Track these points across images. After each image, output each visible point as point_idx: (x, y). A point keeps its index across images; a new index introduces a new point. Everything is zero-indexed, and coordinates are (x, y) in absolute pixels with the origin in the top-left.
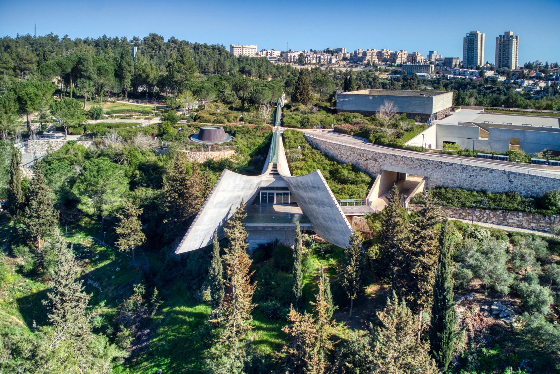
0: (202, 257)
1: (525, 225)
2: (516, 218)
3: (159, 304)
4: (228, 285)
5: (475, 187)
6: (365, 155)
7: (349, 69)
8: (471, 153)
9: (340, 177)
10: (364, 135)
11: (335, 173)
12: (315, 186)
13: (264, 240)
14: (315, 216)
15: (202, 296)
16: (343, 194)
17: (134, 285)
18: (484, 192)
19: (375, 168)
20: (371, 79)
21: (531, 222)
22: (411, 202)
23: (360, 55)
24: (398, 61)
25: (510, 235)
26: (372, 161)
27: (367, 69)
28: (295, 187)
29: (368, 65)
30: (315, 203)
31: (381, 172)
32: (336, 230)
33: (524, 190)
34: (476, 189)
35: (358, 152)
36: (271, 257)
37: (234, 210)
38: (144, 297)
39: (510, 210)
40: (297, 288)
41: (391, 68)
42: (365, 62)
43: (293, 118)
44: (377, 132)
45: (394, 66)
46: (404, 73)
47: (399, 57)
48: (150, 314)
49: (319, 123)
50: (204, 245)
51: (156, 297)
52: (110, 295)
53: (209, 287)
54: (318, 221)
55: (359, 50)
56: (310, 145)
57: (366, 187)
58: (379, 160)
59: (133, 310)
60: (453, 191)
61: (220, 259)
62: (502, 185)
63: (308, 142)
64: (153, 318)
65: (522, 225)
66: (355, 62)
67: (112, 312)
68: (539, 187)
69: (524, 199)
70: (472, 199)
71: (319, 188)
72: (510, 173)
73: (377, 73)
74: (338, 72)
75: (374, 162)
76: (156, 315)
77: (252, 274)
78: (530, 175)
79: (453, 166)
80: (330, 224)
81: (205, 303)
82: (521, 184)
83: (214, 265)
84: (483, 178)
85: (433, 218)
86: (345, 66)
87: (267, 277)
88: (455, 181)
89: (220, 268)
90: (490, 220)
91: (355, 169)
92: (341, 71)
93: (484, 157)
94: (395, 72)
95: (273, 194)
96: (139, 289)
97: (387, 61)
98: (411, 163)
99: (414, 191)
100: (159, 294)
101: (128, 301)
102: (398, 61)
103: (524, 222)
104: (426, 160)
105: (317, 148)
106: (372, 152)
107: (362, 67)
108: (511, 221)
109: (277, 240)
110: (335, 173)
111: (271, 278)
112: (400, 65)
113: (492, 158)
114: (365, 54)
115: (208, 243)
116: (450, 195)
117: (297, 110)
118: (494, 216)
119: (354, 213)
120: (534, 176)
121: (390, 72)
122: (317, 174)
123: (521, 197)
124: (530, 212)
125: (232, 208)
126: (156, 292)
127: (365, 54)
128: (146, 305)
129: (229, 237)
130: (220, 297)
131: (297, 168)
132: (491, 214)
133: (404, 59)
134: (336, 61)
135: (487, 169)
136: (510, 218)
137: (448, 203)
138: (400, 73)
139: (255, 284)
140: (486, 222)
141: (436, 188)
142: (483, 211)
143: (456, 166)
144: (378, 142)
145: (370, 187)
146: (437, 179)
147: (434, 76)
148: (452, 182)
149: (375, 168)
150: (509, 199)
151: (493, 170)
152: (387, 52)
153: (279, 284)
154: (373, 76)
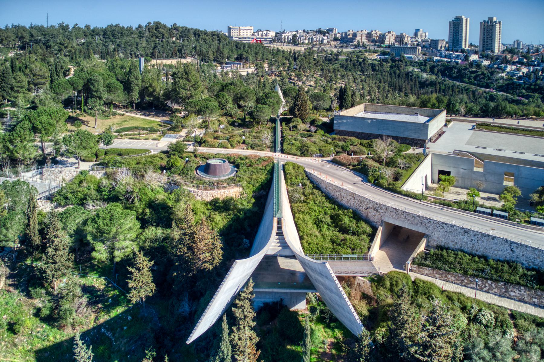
1: (527, 299)
2: (518, 292)
5: (477, 251)
6: (366, 203)
7: (340, 50)
8: (471, 207)
9: (342, 224)
10: (361, 170)
11: (336, 219)
16: (345, 247)
18: (485, 258)
20: (361, 60)
21: (532, 297)
22: (413, 262)
24: (387, 42)
25: (513, 316)
27: (357, 50)
31: (383, 223)
33: (526, 261)
34: (478, 253)
39: (512, 283)
42: (355, 43)
43: (293, 144)
44: (376, 170)
45: (382, 47)
46: (392, 55)
47: (388, 38)
49: (318, 152)
55: (349, 31)
56: (311, 182)
57: (368, 240)
60: (454, 254)
62: (504, 253)
63: (309, 179)
65: (523, 299)
66: (346, 43)
68: (541, 260)
69: (526, 272)
70: (474, 266)
72: (512, 243)
73: (367, 54)
74: (329, 52)
78: (532, 248)
79: (455, 228)
82: (523, 255)
83: (223, 348)
84: (484, 244)
86: (336, 47)
88: (456, 243)
90: (492, 290)
91: (357, 216)
92: (332, 52)
93: (484, 213)
94: (384, 53)
97: (376, 42)
98: (412, 219)
99: (416, 250)
102: (387, 42)
103: (526, 296)
104: (427, 219)
105: (317, 188)
106: (373, 202)
107: (353, 47)
108: (512, 294)
109: (281, 299)
110: (336, 219)
112: (389, 47)
113: (492, 214)
114: (355, 35)
116: (451, 259)
117: (295, 127)
118: (496, 287)
119: (356, 273)
120: (535, 249)
121: (379, 53)
123: (523, 268)
124: (532, 288)
127: (355, 35)
131: (299, 211)
132: (493, 285)
133: (392, 41)
134: (328, 42)
135: (489, 236)
136: (512, 291)
138: (388, 54)
140: (487, 292)
142: (485, 281)
143: (458, 228)
145: (371, 240)
146: (438, 238)
147: (421, 58)
148: (453, 243)
150: (511, 271)
151: (495, 237)
152: (376, 33)
154: (363, 57)
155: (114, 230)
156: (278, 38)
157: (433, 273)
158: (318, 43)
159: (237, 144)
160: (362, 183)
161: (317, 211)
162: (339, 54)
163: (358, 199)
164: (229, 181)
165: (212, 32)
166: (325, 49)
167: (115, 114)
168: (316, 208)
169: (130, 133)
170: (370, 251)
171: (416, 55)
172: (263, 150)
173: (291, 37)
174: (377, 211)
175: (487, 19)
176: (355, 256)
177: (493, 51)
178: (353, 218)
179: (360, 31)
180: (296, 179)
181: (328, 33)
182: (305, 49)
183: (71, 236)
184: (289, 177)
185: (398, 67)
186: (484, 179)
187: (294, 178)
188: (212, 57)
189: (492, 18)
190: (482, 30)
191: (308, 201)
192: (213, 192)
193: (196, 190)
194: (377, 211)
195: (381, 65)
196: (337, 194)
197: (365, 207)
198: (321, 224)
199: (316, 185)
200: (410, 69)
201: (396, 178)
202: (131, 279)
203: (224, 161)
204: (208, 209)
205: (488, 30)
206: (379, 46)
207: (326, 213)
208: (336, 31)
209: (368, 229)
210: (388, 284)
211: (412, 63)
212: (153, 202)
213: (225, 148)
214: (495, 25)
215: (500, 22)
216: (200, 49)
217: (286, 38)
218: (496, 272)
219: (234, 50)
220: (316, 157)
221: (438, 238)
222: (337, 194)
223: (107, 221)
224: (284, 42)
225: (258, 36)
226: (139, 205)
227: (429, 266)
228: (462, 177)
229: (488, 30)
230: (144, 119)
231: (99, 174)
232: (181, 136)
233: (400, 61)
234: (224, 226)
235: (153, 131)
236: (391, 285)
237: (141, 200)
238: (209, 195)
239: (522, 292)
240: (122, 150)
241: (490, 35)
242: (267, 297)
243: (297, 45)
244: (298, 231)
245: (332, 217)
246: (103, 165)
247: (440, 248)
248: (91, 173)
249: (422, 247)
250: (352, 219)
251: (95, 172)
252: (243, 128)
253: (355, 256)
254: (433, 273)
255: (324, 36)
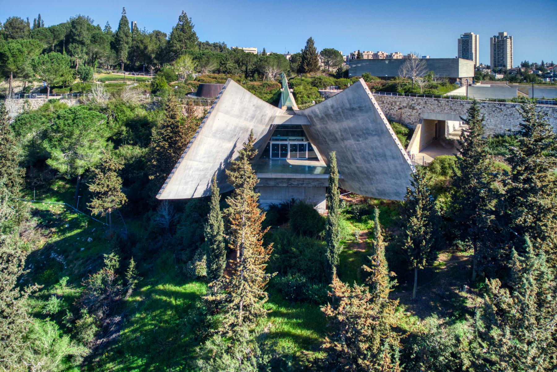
0: (197, 222)
3: (136, 281)
4: (232, 247)
12: (355, 106)
13: (277, 199)
14: (350, 158)
15: (194, 269)
17: (105, 255)
19: (412, 118)
26: (407, 109)
28: (322, 119)
30: (352, 135)
32: (385, 173)
35: (388, 101)
36: (286, 220)
37: (240, 147)
38: (117, 271)
40: (332, 252)
43: (302, 80)
44: (405, 85)
48: (125, 292)
49: (333, 84)
50: (199, 194)
51: (132, 271)
52: (76, 271)
53: (205, 257)
54: (353, 166)
58: (418, 107)
59: (101, 289)
61: (219, 212)
64: (128, 301)
67: (75, 293)
71: (361, 109)
75: (411, 110)
76: (132, 295)
77: (266, 231)
80: (375, 165)
81: (200, 279)
83: (212, 221)
85: (541, 140)
87: (285, 242)
89: (220, 225)
95: (286, 146)
96: (112, 260)
100: (136, 267)
101: (95, 275)
109: (293, 199)
111: (290, 244)
115: (205, 192)
122: (361, 85)
125: (238, 145)
126: (133, 264)
128: (120, 283)
129: (233, 182)
130: (219, 268)
139: (270, 247)
141: (497, 136)
144: (409, 92)
146: (496, 125)
149: (412, 118)
153: (301, 252)
155: (77, 132)
163: (388, 101)
165: (214, 44)
170: (409, 147)
175: (497, 35)
177: (505, 66)
179: (366, 52)
180: (309, 97)
183: (24, 147)
184: (300, 96)
189: (503, 33)
190: (493, 46)
202: (94, 183)
205: (499, 46)
209: (404, 130)
212: (133, 120)
214: (506, 40)
215: (511, 37)
223: (70, 121)
226: (114, 125)
229: (499, 46)
237: (117, 120)
241: (502, 51)
242: (274, 197)
251: (66, 100)
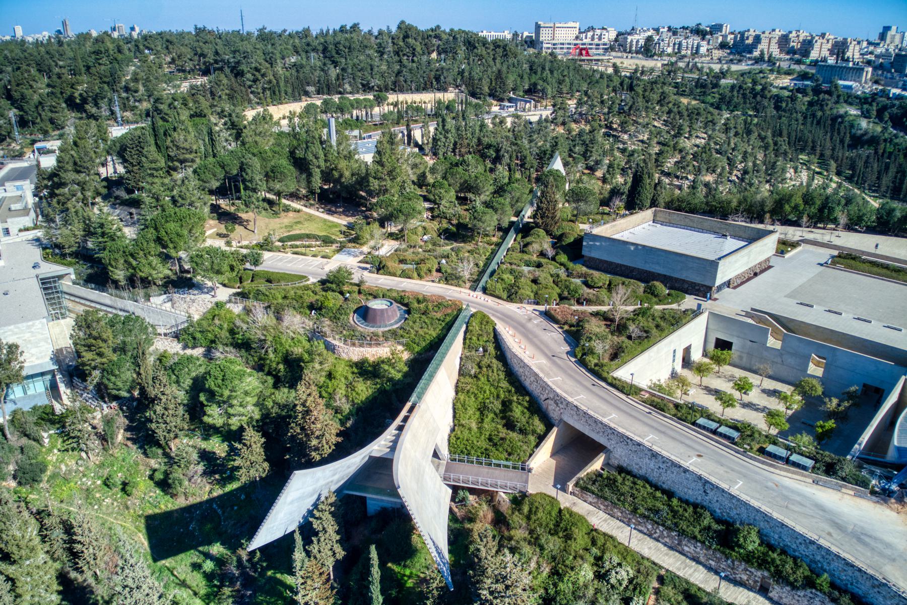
1: (702, 559)
22: (576, 485)
23: (750, 41)
24: (814, 55)
29: (759, 60)
34: (664, 486)
39: (687, 536)
41: (797, 68)
42: (756, 53)
45: (804, 63)
46: (817, 80)
47: (817, 46)
66: (739, 53)
70: (650, 503)
73: (772, 77)
74: (706, 70)
92: (711, 70)
94: (804, 76)
104: (611, 428)
107: (750, 62)
108: (686, 549)
112: (815, 63)
116: (625, 489)
118: (668, 536)
132: (665, 533)
133: (825, 53)
134: (708, 50)
137: (619, 500)
140: (657, 540)
152: (798, 36)
154: (763, 81)
156: (620, 44)
157: (597, 503)
158: (689, 52)
159: (426, 274)
160: (565, 356)
161: (488, 392)
162: (723, 74)
164: (389, 335)
166: (699, 65)
167: (287, 209)
168: (487, 388)
169: (298, 243)
171: (860, 82)
172: (459, 286)
173: (642, 42)
174: (557, 404)
176: (510, 463)
178: (528, 409)
181: (711, 33)
182: (663, 65)
185: (822, 106)
186: (779, 360)
187: (474, 338)
188: (486, 89)
191: (480, 376)
192: (362, 349)
193: (341, 344)
194: (557, 404)
195: (793, 99)
196: (521, 370)
197: (545, 396)
198: (486, 412)
199: (501, 353)
200: (844, 109)
201: (615, 355)
203: (391, 304)
204: (353, 373)
206: (799, 62)
207: (498, 396)
208: (726, 29)
210: (526, 509)
211: (850, 98)
213: (410, 278)
216: (470, 74)
217: (634, 43)
218: (674, 517)
219: (526, 76)
220: (528, 303)
221: (621, 455)
222: (521, 370)
224: (630, 52)
225: (585, 41)
227: (593, 493)
228: (748, 353)
230: (325, 220)
231: (237, 309)
232: (361, 253)
233: (829, 93)
234: (367, 398)
235: (327, 241)
236: (530, 511)
238: (356, 353)
239: (698, 550)
240: (273, 273)
243: (652, 56)
244: (454, 417)
245: (504, 403)
246: (243, 295)
247: (621, 470)
248: (228, 306)
249: (597, 465)
250: (526, 411)
251: (232, 305)
252: (456, 241)
253: (510, 463)
254: (597, 503)
255: (703, 39)
